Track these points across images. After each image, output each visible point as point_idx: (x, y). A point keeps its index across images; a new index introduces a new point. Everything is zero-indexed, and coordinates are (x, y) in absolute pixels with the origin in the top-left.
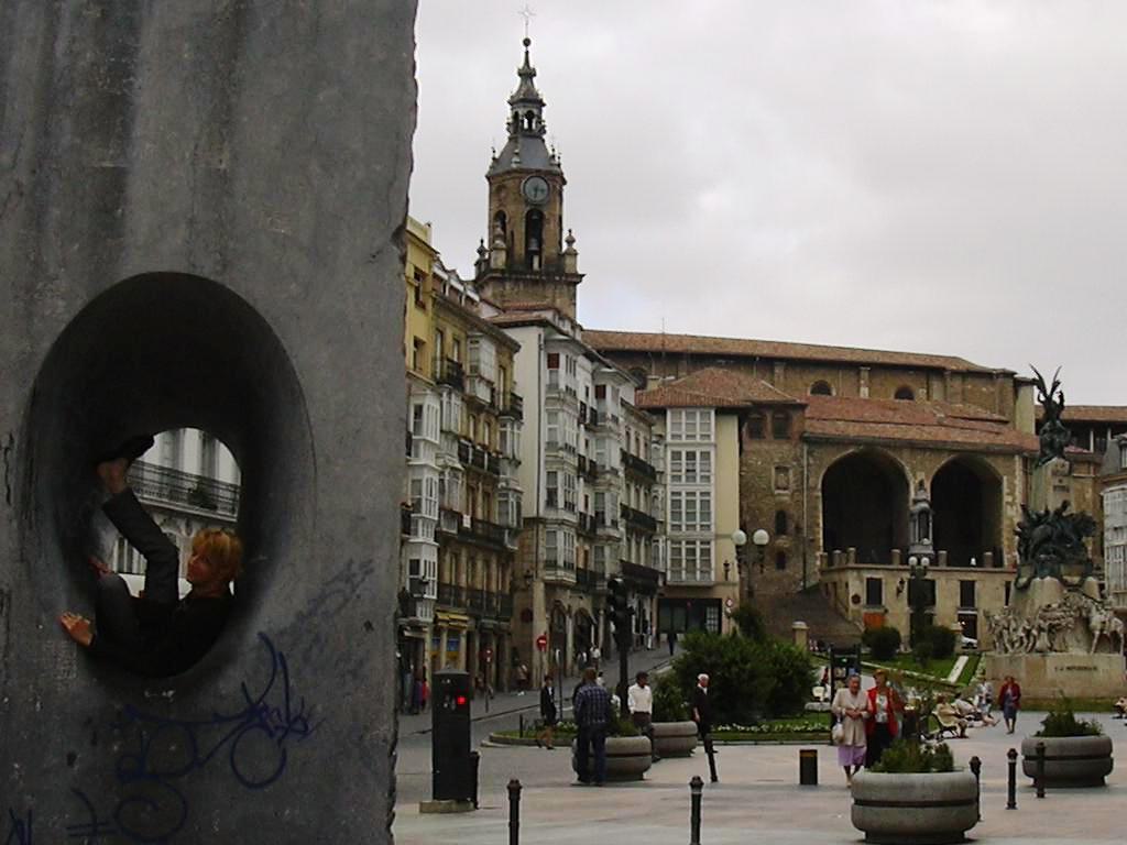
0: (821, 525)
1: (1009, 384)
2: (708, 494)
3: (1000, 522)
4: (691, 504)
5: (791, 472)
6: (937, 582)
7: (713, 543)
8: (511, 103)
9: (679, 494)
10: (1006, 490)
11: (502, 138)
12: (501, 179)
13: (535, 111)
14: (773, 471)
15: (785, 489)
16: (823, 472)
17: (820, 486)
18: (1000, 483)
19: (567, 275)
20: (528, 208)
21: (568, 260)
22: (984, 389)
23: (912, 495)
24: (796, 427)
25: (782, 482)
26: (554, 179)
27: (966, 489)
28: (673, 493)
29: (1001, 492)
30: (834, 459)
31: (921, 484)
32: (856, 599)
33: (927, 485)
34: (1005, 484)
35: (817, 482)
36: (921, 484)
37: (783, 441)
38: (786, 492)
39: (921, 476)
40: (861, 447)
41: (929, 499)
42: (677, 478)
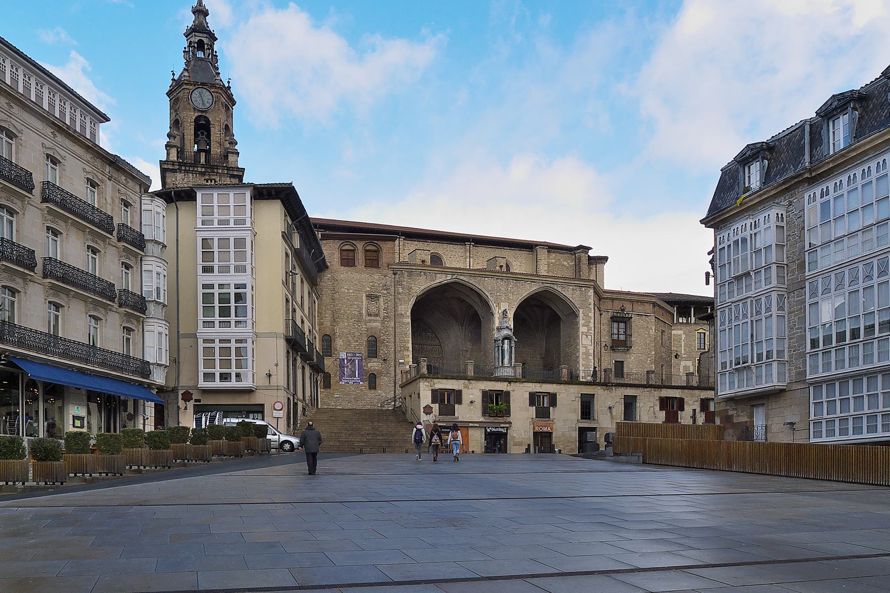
0: (411, 349)
1: (584, 260)
2: (244, 286)
3: (578, 351)
4: (224, 298)
5: (381, 299)
6: (512, 393)
7: (250, 341)
8: (186, 36)
9: (212, 286)
10: (581, 322)
11: (179, 66)
12: (177, 92)
13: (206, 41)
14: (364, 298)
15: (377, 315)
16: (413, 301)
17: (409, 313)
18: (577, 316)
19: (228, 169)
20: (197, 114)
21: (231, 158)
22: (565, 263)
23: (497, 324)
24: (385, 258)
25: (373, 309)
26: (226, 98)
27: (543, 317)
28: (205, 286)
29: (577, 323)
30: (422, 288)
31: (505, 313)
32: (428, 410)
33: (511, 315)
34: (581, 315)
35: (406, 309)
36: (505, 313)
37: (374, 269)
38: (378, 318)
39: (504, 306)
40: (449, 277)
41: (512, 327)
42: (207, 270)
